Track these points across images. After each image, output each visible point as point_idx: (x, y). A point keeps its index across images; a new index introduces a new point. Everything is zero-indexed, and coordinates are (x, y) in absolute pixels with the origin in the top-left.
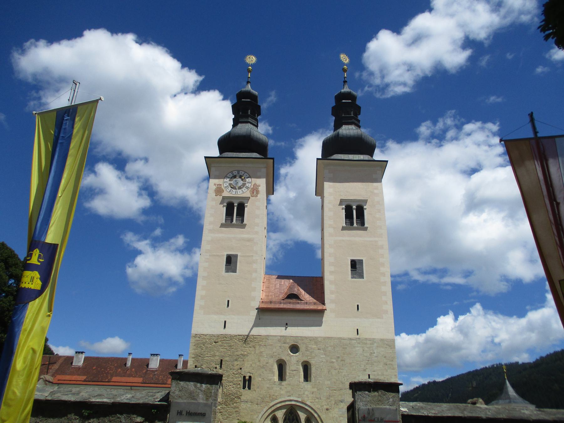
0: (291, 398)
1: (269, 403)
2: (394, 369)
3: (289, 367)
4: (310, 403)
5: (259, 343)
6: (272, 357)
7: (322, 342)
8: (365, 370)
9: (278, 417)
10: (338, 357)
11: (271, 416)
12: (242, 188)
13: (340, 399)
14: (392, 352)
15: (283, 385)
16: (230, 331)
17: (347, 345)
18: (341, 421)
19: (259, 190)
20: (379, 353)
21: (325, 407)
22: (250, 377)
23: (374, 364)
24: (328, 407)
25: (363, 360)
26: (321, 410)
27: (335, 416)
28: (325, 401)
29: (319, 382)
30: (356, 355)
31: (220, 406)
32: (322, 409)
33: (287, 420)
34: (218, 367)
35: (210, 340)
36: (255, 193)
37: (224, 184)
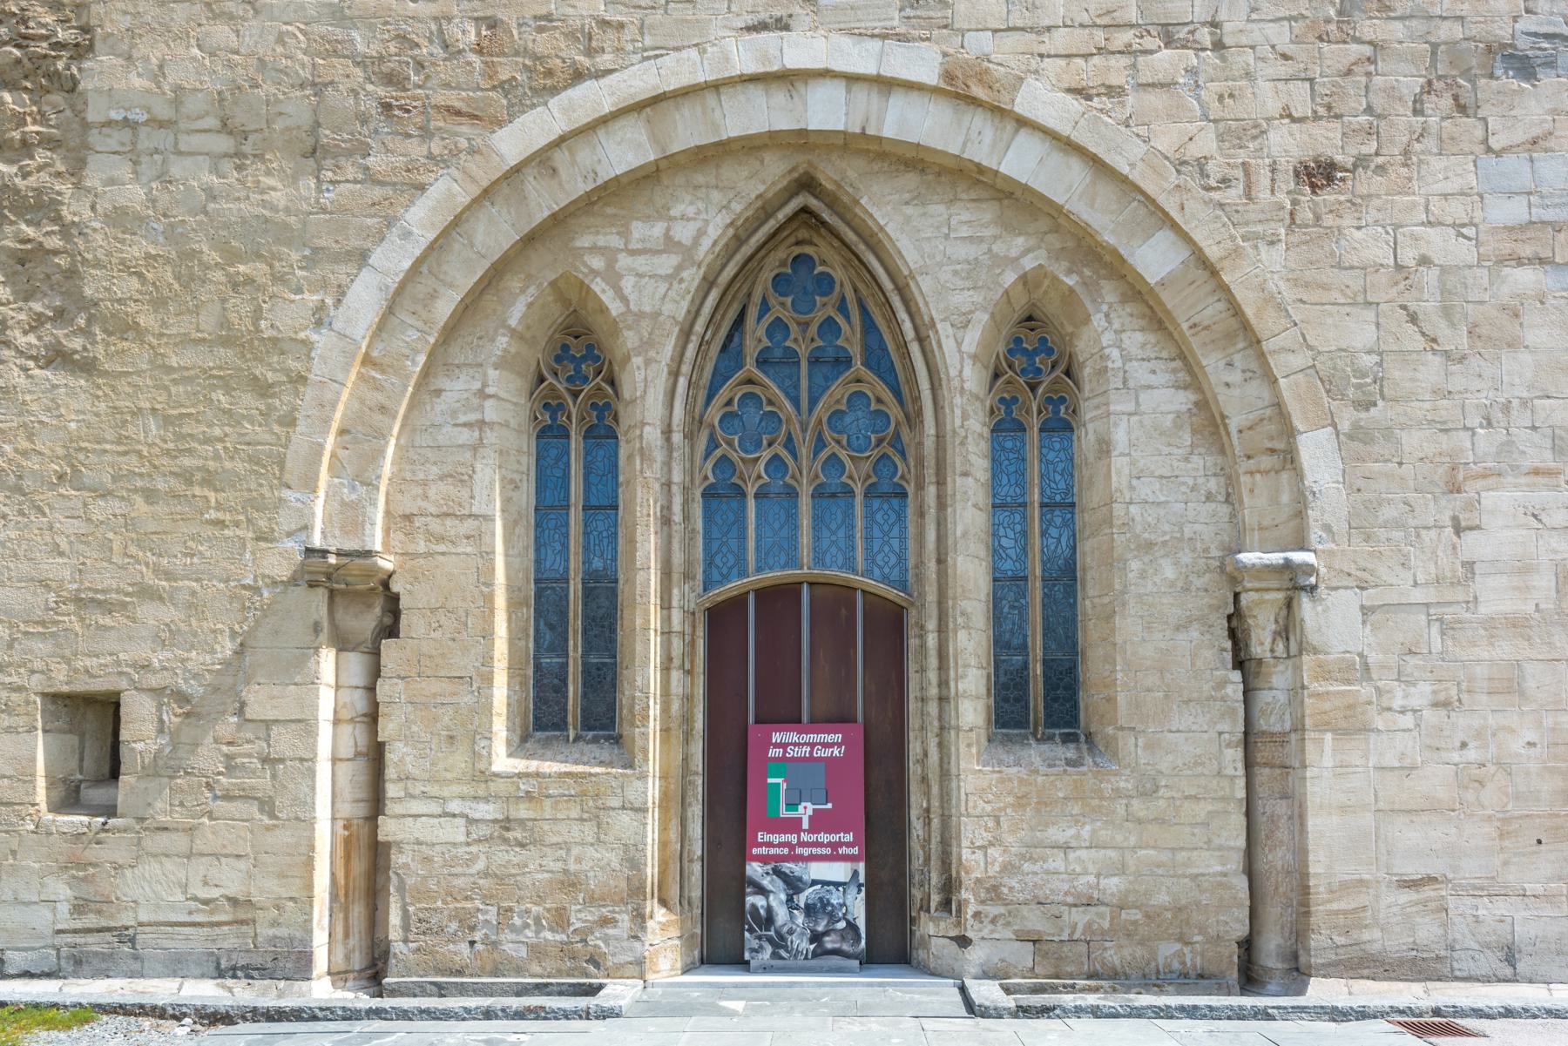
4: (1075, 104)
9: (615, 308)
24: (1327, 141)
26: (1225, 181)
27: (1424, 261)
28: (1283, 69)
32: (1239, 173)
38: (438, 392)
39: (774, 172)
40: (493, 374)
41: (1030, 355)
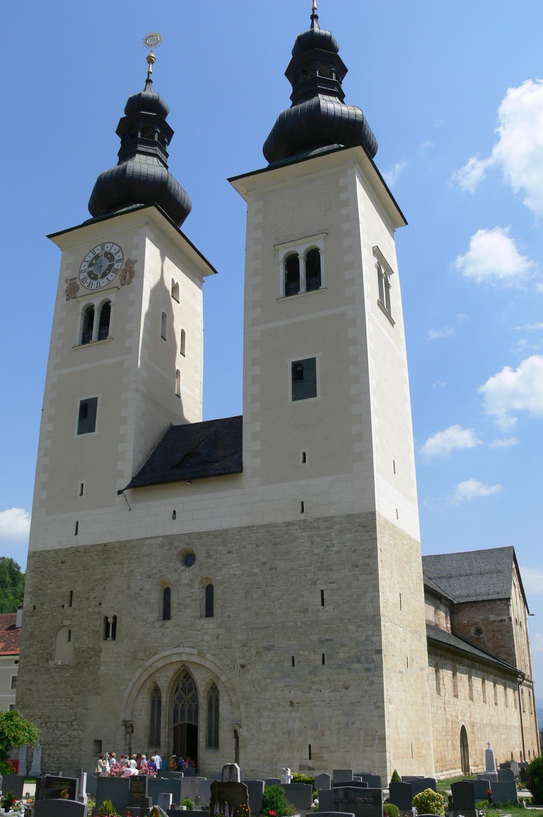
0: (181, 650)
1: (143, 662)
2: (372, 573)
3: (178, 593)
5: (128, 554)
6: (150, 577)
7: (236, 537)
8: (314, 583)
10: (265, 563)
11: (149, 685)
12: (107, 274)
13: (266, 645)
14: (369, 538)
15: (167, 628)
16: (86, 539)
17: (282, 537)
18: (267, 685)
19: (134, 269)
20: (343, 543)
21: (239, 662)
22: (115, 618)
23: (334, 568)
24: (243, 661)
25: (311, 563)
28: (238, 651)
29: (229, 616)
30: (298, 554)
31: (69, 672)
32: (233, 666)
33: (180, 690)
34: (66, 606)
35: (54, 559)
36: (128, 277)
37: (81, 275)
38: (139, 698)
39: (179, 665)
40: (145, 695)
41: (214, 689)
